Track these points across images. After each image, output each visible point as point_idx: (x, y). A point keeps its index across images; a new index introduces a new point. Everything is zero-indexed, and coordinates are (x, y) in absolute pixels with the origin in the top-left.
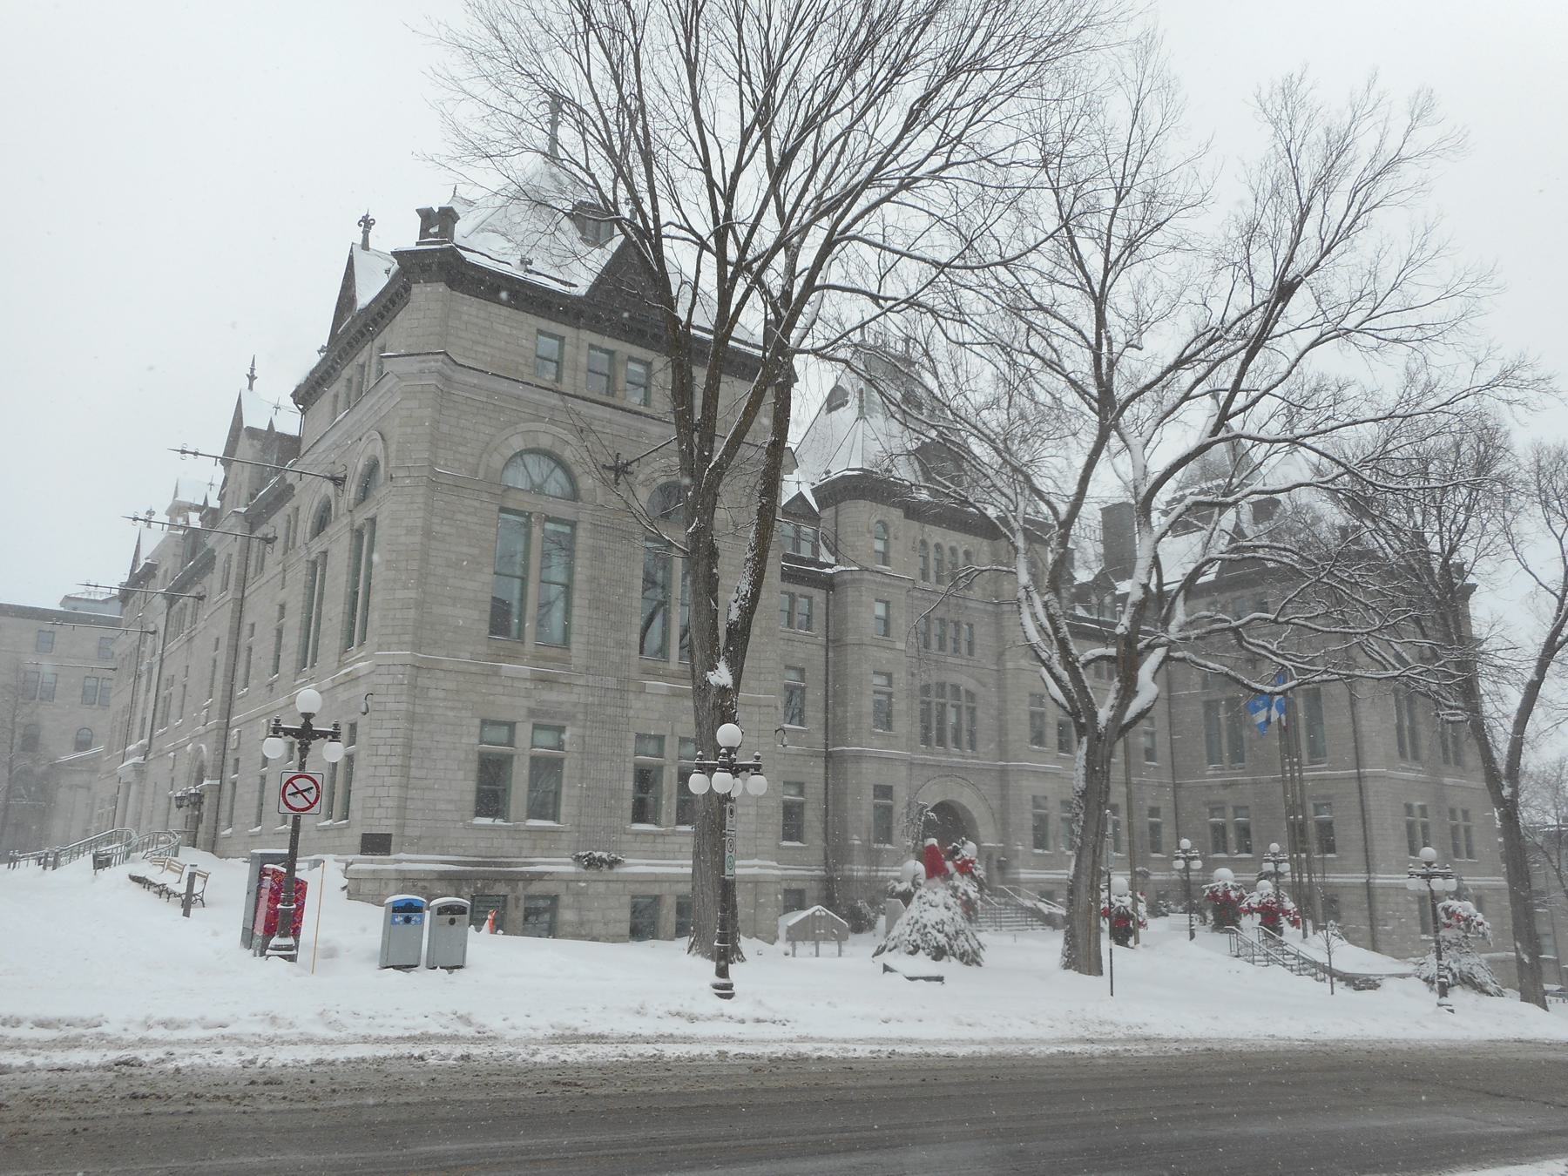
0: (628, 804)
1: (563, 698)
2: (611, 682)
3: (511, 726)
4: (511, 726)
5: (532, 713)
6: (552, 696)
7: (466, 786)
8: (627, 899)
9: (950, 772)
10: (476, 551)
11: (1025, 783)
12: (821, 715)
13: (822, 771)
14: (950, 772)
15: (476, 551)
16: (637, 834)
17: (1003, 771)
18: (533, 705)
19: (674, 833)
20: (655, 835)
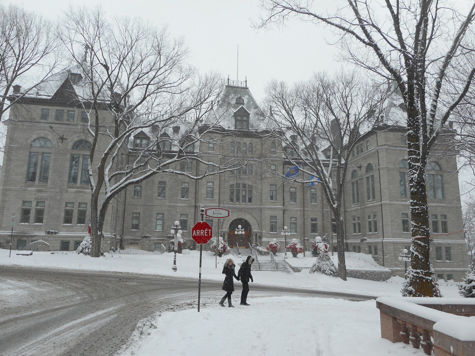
0: (62, 219)
1: (44, 195)
2: (58, 190)
3: (31, 202)
4: (31, 202)
5: (36, 199)
6: (41, 194)
7: (18, 216)
8: (59, 241)
9: (241, 210)
10: (22, 163)
11: (266, 212)
12: (194, 195)
13: (194, 211)
14: (241, 210)
15: (22, 163)
16: (64, 226)
17: (261, 210)
18: (36, 197)
19: (75, 226)
20: (70, 226)
